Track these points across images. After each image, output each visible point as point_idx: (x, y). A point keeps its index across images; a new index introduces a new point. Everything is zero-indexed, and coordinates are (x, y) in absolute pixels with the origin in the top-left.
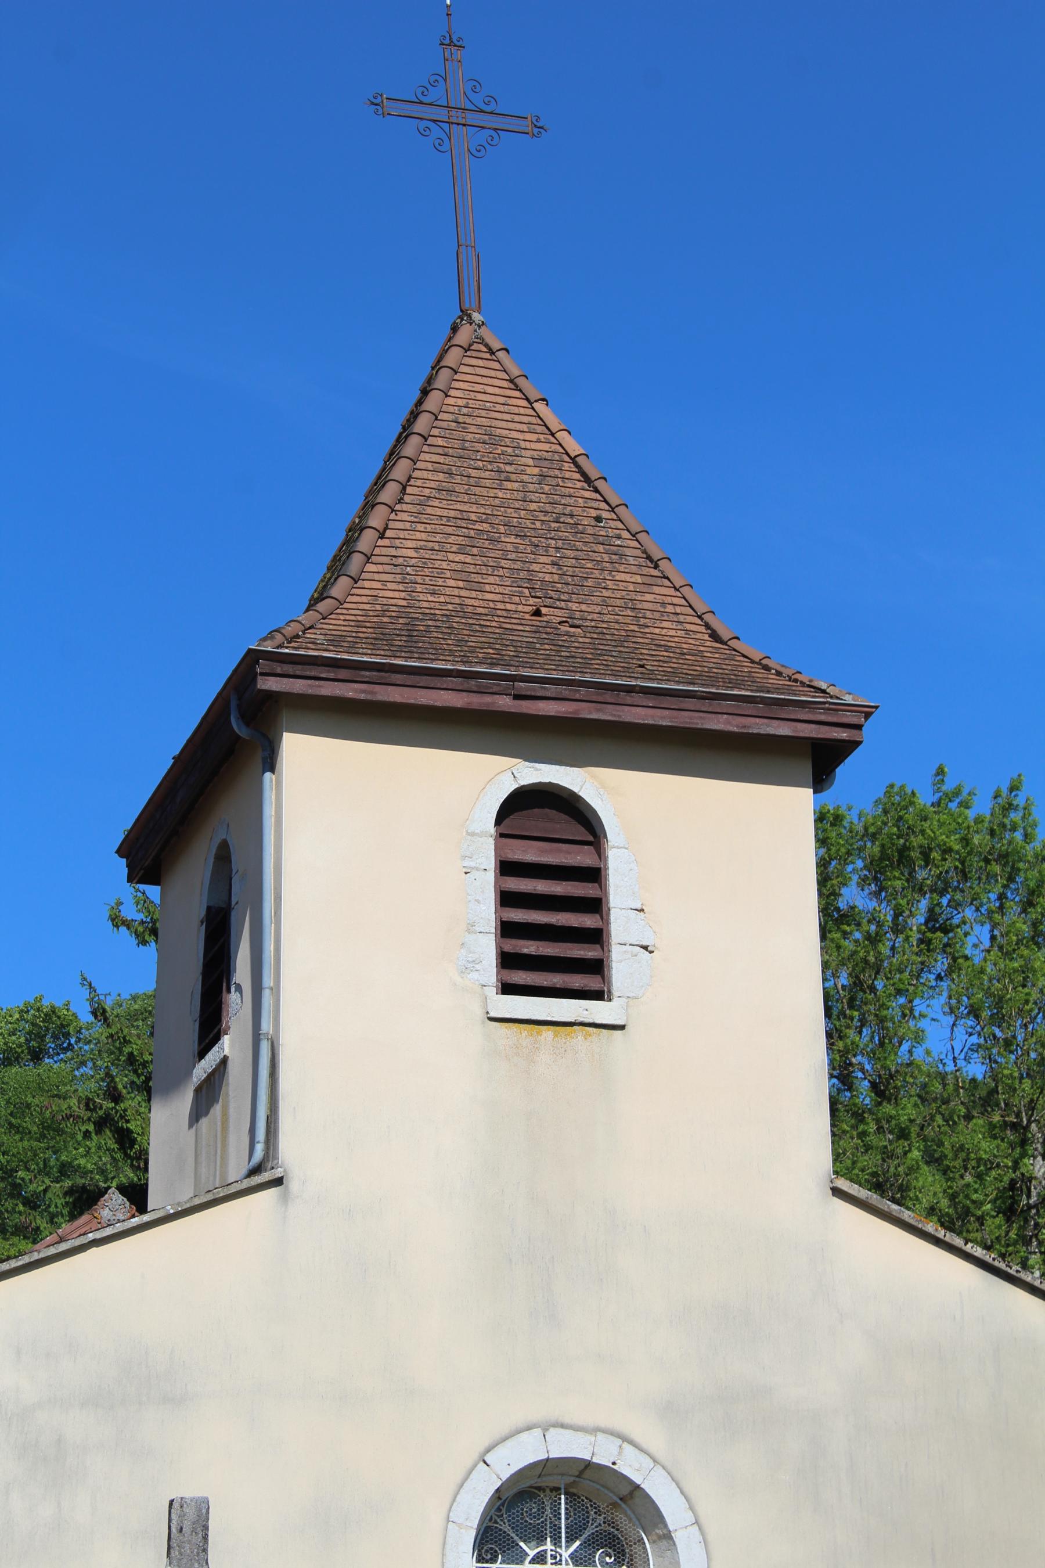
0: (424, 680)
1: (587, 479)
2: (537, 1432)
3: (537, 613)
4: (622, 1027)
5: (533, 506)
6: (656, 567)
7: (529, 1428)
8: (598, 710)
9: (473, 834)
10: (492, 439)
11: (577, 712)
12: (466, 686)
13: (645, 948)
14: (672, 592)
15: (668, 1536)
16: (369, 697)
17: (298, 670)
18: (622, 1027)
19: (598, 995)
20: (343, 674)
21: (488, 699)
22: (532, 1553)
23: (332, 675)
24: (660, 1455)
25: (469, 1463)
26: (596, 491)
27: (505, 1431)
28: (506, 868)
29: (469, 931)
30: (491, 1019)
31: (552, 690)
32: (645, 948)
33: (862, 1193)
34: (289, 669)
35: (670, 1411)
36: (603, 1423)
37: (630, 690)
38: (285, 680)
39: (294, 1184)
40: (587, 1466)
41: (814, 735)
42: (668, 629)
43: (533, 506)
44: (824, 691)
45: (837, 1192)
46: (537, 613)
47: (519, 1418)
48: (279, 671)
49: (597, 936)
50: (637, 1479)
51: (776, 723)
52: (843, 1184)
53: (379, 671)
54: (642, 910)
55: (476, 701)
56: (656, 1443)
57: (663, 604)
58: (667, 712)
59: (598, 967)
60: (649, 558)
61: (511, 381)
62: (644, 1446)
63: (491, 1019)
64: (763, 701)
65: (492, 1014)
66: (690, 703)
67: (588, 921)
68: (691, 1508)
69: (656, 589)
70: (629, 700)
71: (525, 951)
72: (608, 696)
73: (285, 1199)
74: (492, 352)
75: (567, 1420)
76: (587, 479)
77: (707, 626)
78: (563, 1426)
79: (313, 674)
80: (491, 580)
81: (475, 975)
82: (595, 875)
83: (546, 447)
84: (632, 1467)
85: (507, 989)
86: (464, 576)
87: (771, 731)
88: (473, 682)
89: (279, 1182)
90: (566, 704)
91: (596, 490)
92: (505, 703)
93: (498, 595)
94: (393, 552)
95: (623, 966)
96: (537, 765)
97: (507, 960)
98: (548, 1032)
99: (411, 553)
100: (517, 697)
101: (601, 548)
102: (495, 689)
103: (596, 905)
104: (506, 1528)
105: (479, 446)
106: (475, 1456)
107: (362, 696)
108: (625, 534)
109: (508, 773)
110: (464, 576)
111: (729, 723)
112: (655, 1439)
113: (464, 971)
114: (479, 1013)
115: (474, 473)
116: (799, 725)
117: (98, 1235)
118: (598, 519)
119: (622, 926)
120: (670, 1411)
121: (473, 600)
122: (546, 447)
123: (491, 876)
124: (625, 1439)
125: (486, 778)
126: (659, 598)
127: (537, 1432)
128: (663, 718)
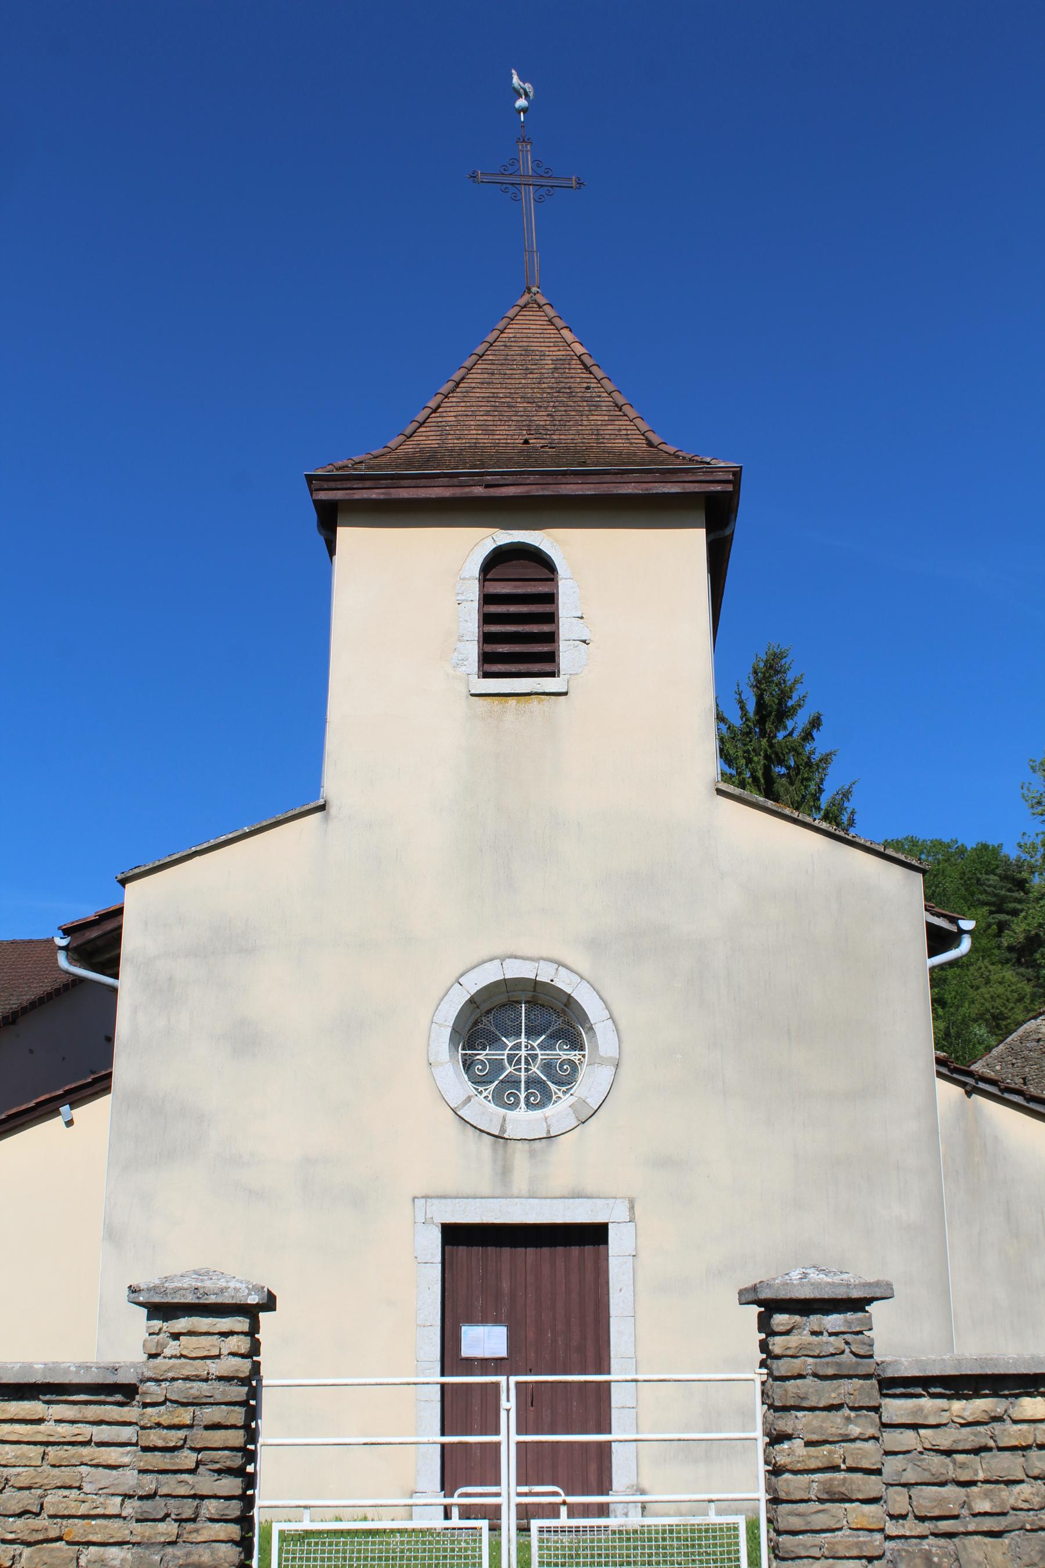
0: (423, 482)
1: (586, 367)
2: (497, 962)
3: (526, 442)
4: (566, 694)
5: (544, 386)
6: (620, 410)
7: (491, 960)
8: (543, 489)
9: (464, 579)
10: (527, 352)
11: (528, 492)
12: (451, 483)
13: (584, 642)
14: (628, 423)
15: (591, 1028)
16: (386, 497)
17: (339, 485)
18: (566, 694)
19: (552, 674)
20: (368, 484)
21: (467, 490)
22: (510, 1045)
23: (360, 486)
24: (586, 973)
25: (449, 984)
26: (591, 373)
27: (475, 962)
28: (487, 599)
29: (460, 641)
30: (472, 695)
31: (510, 479)
32: (584, 642)
33: (737, 791)
34: (332, 484)
35: (595, 945)
36: (544, 954)
37: (564, 473)
38: (330, 492)
39: (333, 810)
40: (535, 985)
41: (697, 490)
42: (619, 444)
43: (544, 386)
44: (708, 463)
45: (720, 792)
46: (526, 442)
47: (485, 953)
48: (326, 486)
49: (551, 638)
50: (568, 990)
51: (669, 485)
52: (724, 786)
53: (392, 479)
54: (582, 618)
55: (458, 492)
56: (583, 967)
57: (620, 430)
58: (592, 486)
59: (551, 657)
60: (617, 406)
61: (549, 321)
62: (574, 967)
63: (472, 695)
64: (658, 471)
65: (473, 692)
66: (608, 478)
67: (546, 628)
68: (607, 1008)
69: (617, 423)
70: (565, 481)
71: (500, 650)
72: (550, 479)
73: (326, 819)
74: (540, 307)
75: (519, 953)
76: (586, 367)
77: (647, 439)
78: (516, 957)
79: (348, 486)
80: (502, 428)
81: (463, 668)
82: (551, 598)
83: (564, 353)
84: (564, 982)
85: (486, 675)
86: (484, 428)
87: (666, 490)
88: (455, 480)
89: (322, 808)
90: (525, 490)
91: (591, 373)
92: (479, 491)
93: (507, 435)
94: (440, 419)
95: (567, 654)
96: (510, 532)
97: (486, 658)
98: (512, 702)
99: (453, 419)
100: (487, 486)
101: (585, 404)
102: (471, 483)
103: (551, 618)
104: (493, 1029)
105: (518, 358)
106: (453, 979)
107: (382, 497)
108: (605, 394)
109: (486, 539)
110: (484, 428)
111: (636, 488)
112: (581, 961)
113: (456, 666)
114: (464, 691)
115: (508, 372)
116: (686, 485)
117: (198, 848)
118: (588, 388)
119: (567, 628)
120: (595, 945)
121: (485, 440)
122: (564, 353)
123: (476, 605)
124: (560, 964)
125: (477, 542)
126: (617, 427)
127: (497, 962)
128: (589, 490)
